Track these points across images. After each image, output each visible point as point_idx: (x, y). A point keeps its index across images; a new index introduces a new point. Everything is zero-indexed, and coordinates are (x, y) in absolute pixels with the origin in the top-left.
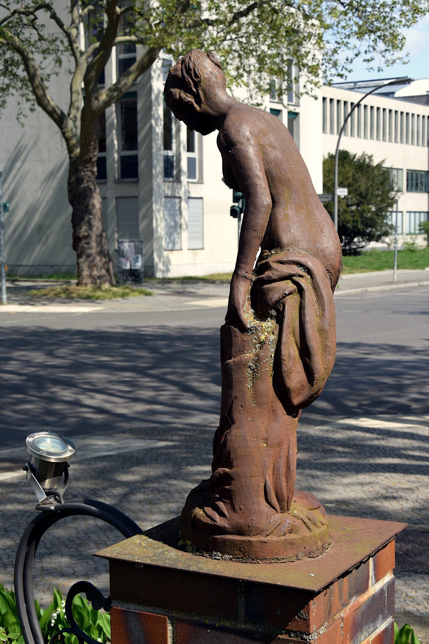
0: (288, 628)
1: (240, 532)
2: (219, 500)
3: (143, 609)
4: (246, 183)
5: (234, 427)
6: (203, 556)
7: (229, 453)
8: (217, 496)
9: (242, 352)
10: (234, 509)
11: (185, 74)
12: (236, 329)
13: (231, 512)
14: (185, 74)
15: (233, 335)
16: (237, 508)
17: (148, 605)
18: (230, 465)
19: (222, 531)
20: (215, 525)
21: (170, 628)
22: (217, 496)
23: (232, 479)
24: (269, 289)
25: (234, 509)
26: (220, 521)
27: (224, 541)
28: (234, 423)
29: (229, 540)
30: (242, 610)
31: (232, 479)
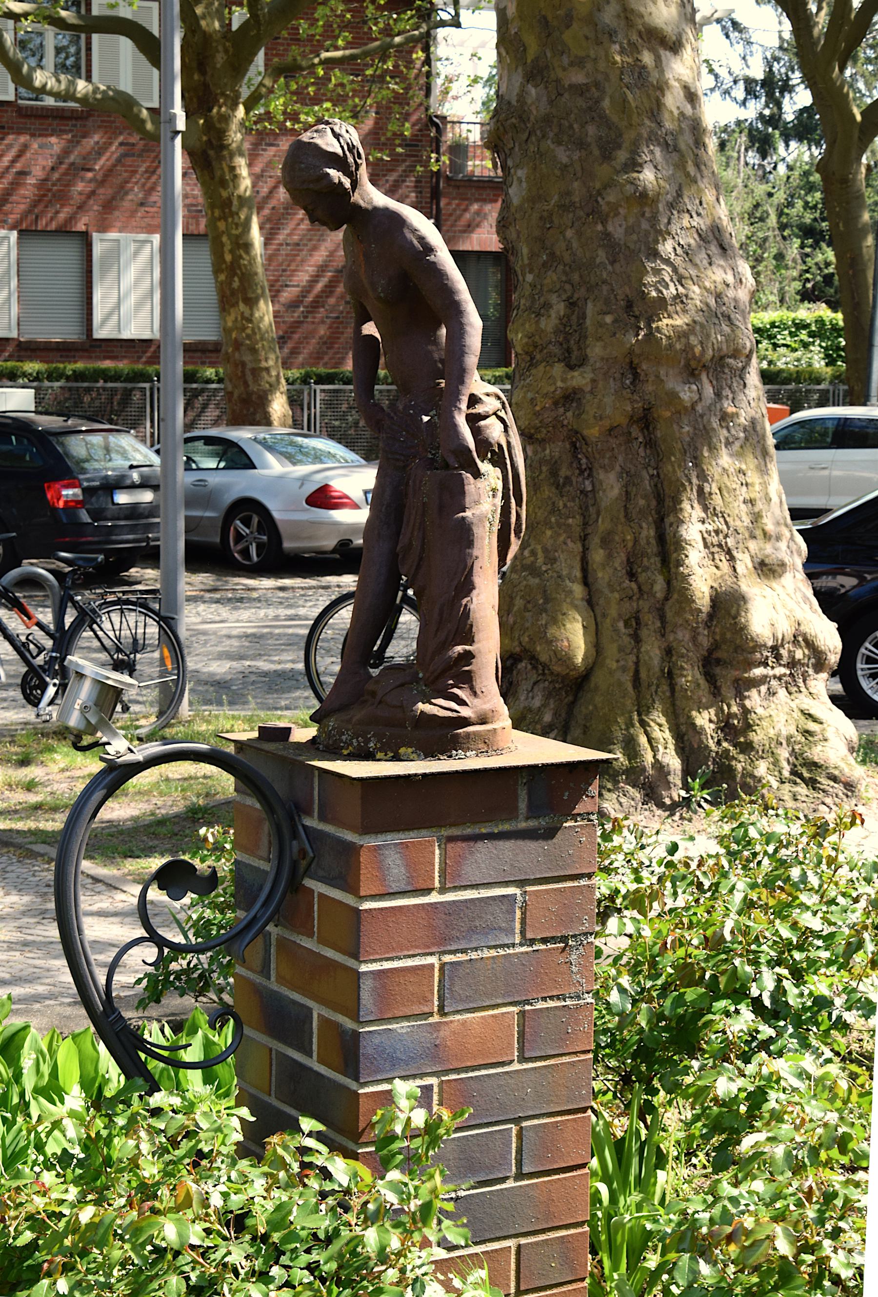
0: (575, 812)
1: (483, 721)
2: (453, 686)
3: (403, 836)
4: (457, 298)
5: (475, 592)
6: (450, 756)
7: (472, 626)
8: (451, 682)
9: (477, 502)
10: (475, 694)
11: (347, 153)
12: (469, 475)
13: (472, 698)
14: (347, 153)
15: (466, 482)
16: (479, 692)
17: (409, 830)
18: (470, 640)
19: (465, 722)
20: (460, 717)
21: (437, 852)
22: (451, 682)
23: (474, 657)
24: (487, 427)
25: (475, 694)
26: (465, 712)
27: (468, 735)
28: (474, 588)
29: (474, 733)
30: (523, 805)
31: (474, 657)
